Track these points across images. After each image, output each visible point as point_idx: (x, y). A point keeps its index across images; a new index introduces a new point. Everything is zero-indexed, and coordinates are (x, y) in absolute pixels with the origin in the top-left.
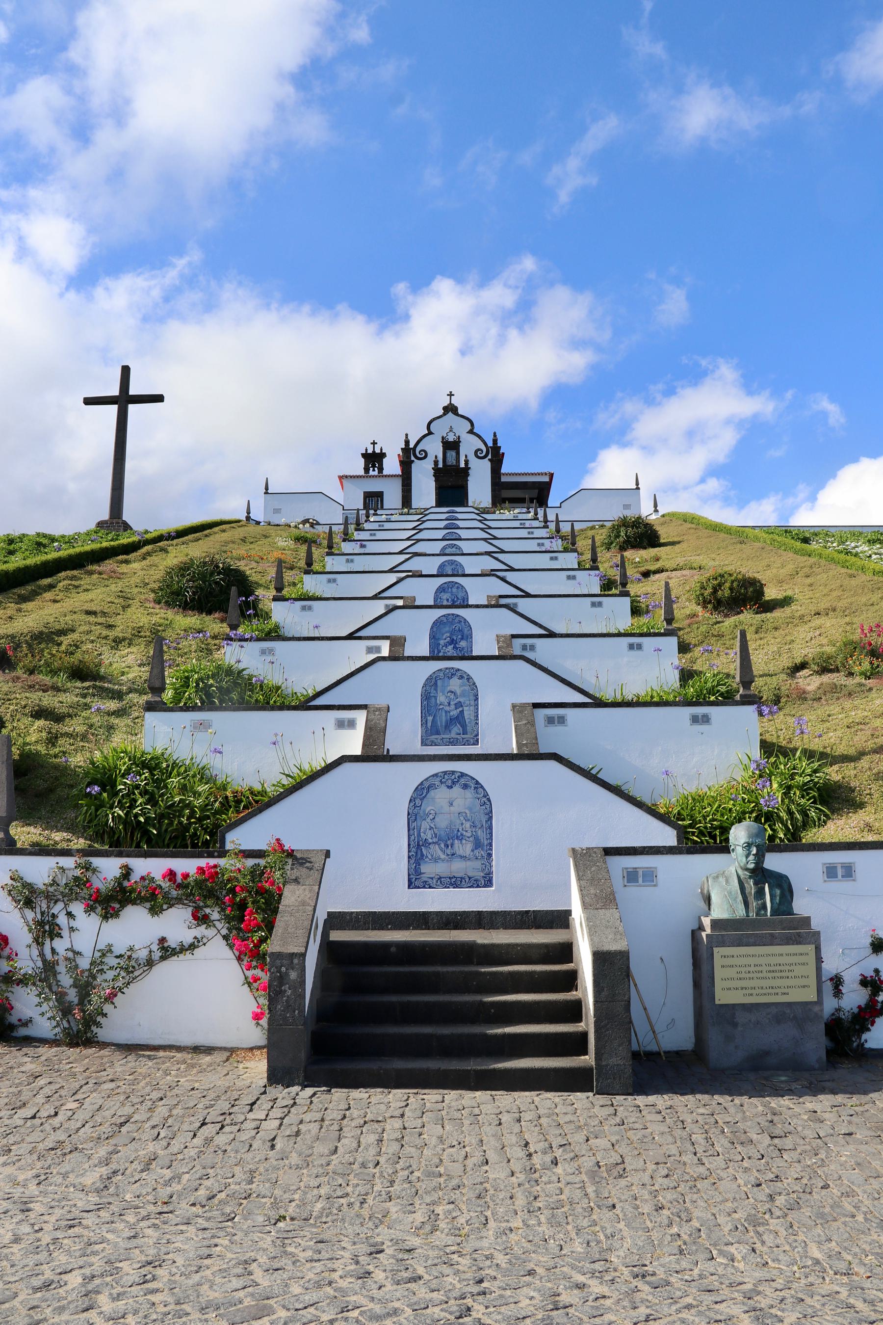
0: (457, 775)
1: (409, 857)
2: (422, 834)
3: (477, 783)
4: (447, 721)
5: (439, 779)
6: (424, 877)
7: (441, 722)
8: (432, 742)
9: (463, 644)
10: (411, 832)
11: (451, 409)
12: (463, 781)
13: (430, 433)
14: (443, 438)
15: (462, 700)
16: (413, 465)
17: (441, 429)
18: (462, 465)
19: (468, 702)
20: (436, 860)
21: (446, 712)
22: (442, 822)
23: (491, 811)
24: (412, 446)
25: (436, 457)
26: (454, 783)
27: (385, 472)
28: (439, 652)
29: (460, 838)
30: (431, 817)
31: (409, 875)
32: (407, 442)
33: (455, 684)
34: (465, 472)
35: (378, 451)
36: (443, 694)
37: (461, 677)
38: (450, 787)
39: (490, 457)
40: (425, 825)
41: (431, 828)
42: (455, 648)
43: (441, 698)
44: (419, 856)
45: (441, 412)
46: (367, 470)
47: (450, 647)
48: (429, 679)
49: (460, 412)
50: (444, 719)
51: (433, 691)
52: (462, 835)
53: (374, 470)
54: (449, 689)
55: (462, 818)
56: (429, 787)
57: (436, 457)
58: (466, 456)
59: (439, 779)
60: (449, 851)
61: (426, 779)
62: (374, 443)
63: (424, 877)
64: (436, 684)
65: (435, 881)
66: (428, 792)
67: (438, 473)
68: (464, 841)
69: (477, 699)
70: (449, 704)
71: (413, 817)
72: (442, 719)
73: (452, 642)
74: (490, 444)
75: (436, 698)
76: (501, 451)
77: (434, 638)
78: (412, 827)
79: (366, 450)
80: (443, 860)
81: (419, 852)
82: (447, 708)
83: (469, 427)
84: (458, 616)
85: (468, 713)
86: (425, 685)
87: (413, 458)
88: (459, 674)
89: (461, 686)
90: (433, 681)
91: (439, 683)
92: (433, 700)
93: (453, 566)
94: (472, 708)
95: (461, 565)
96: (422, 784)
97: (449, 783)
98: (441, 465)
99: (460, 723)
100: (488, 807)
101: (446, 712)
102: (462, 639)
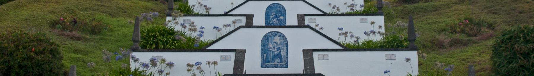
4: (273, 56)
7: (270, 57)
8: (266, 66)
9: (282, 18)
15: (280, 46)
19: (283, 48)
21: (273, 52)
28: (270, 21)
33: (277, 39)
36: (271, 44)
37: (280, 36)
42: (278, 20)
43: (270, 46)
47: (275, 19)
48: (265, 36)
50: (272, 56)
54: (274, 41)
64: (268, 39)
69: (287, 46)
70: (274, 48)
72: (271, 55)
73: (276, 17)
75: (268, 45)
77: (267, 14)
82: (273, 50)
84: (279, 4)
85: (283, 53)
86: (263, 39)
88: (279, 34)
89: (280, 40)
90: (267, 37)
91: (270, 38)
94: (285, 50)
99: (279, 57)
101: (273, 52)
102: (281, 15)
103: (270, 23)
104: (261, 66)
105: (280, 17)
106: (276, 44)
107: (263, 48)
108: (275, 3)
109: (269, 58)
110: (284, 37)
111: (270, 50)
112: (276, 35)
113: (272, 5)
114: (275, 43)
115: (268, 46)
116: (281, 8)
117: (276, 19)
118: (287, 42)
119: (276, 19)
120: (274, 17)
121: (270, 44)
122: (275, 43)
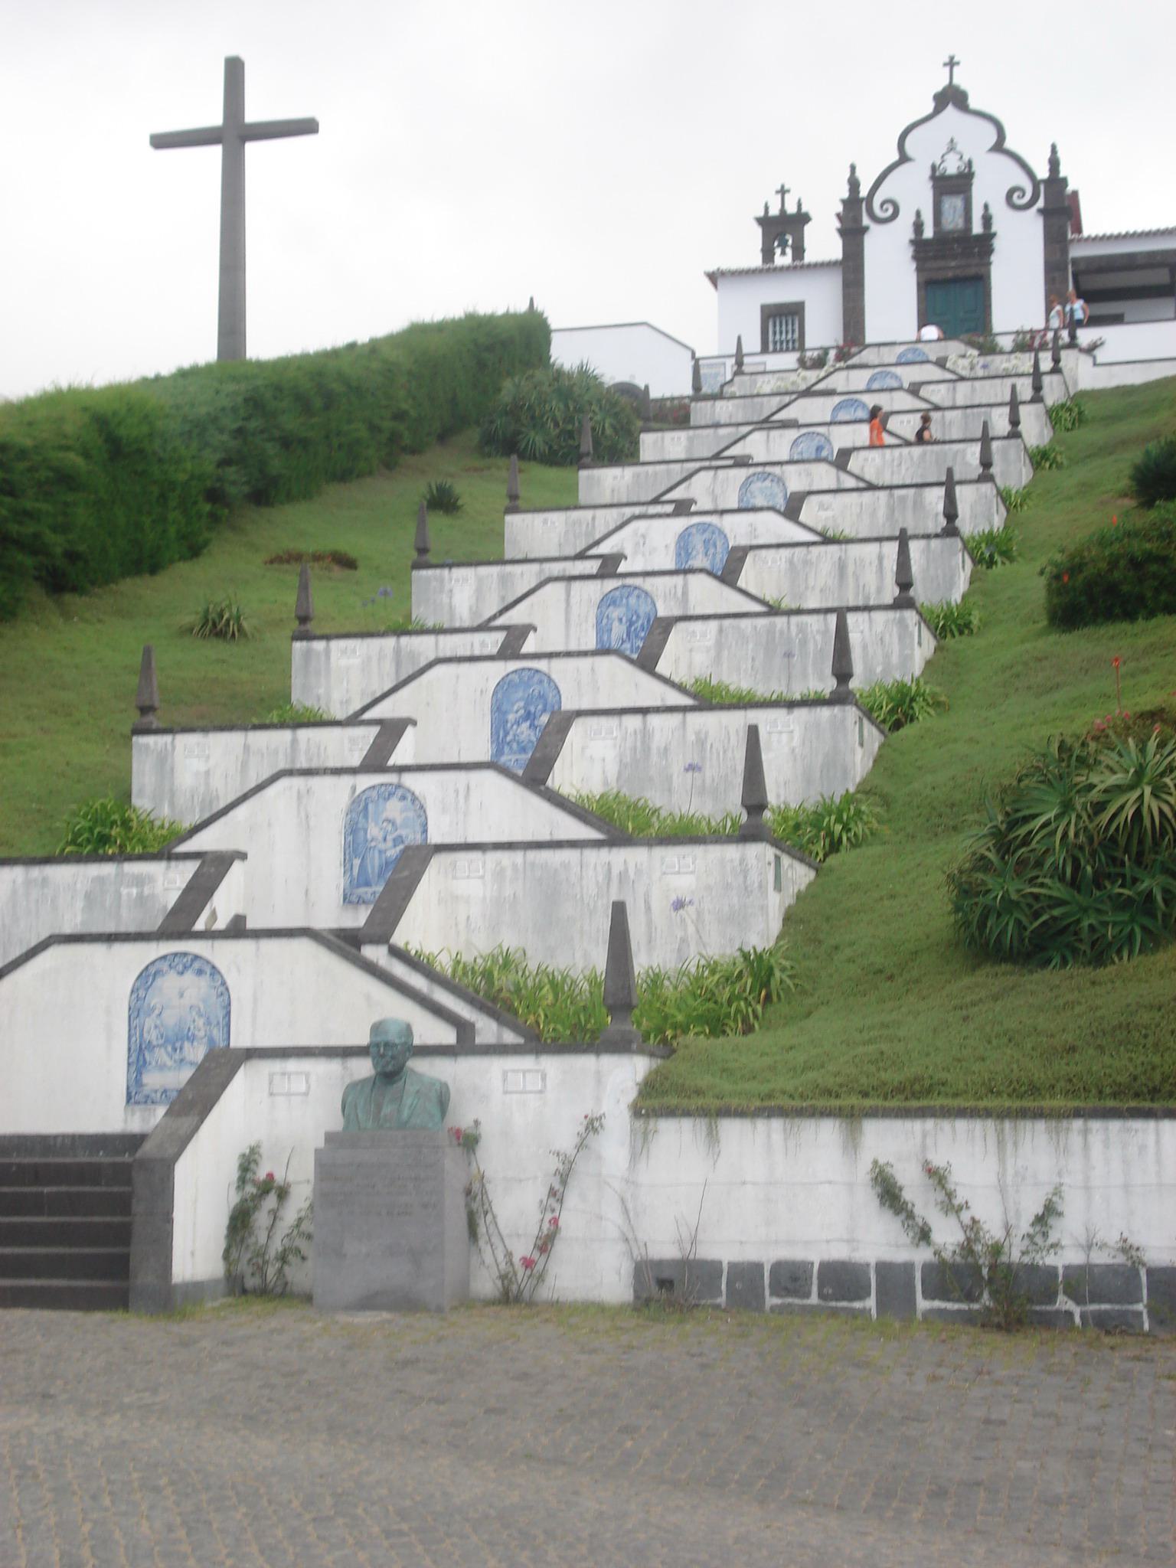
0: (190, 958)
1: (129, 1064)
2: (145, 1035)
3: (214, 967)
4: (381, 867)
5: (167, 963)
6: (146, 1090)
7: (373, 867)
10: (133, 1032)
11: (951, 98)
12: (196, 965)
13: (904, 158)
14: (934, 168)
16: (869, 241)
17: (927, 149)
18: (977, 228)
20: (162, 1067)
21: (380, 852)
22: (170, 1019)
23: (230, 1004)
24: (864, 192)
25: (918, 214)
26: (186, 968)
27: (809, 257)
28: (506, 734)
29: (192, 1039)
30: (157, 1012)
31: (128, 1088)
32: (854, 184)
33: (394, 808)
34: (983, 245)
35: (791, 209)
36: (376, 824)
37: (403, 798)
38: (182, 973)
39: (1041, 203)
40: (149, 1023)
41: (156, 1027)
42: (532, 726)
43: (374, 831)
44: (141, 1063)
45: (930, 107)
46: (768, 254)
47: (525, 725)
49: (973, 103)
50: (377, 862)
51: (361, 820)
52: (193, 1035)
53: (783, 253)
54: (384, 816)
55: (194, 1013)
56: (155, 974)
57: (918, 214)
58: (986, 207)
59: (167, 963)
60: (177, 1056)
61: (153, 963)
62: (783, 192)
63: (146, 1090)
64: (366, 808)
65: (159, 1094)
66: (154, 980)
67: (924, 251)
68: (195, 1044)
70: (385, 839)
71: (136, 1012)
74: (1042, 172)
76: (1070, 188)
78: (133, 1026)
79: (767, 209)
80: (170, 1069)
81: (141, 1058)
82: (382, 846)
83: (992, 138)
84: (537, 671)
86: (350, 811)
87: (866, 221)
89: (402, 812)
90: (362, 804)
91: (371, 807)
92: (362, 833)
93: (707, 535)
95: (721, 532)
96: (147, 968)
97: (180, 967)
98: (928, 233)
100: (226, 998)
101: (380, 852)
103: (509, 738)
104: (344, 899)
105: (540, 716)
106: (390, 825)
107: (350, 838)
108: (523, 669)
109: (370, 871)
110: (417, 802)
111: (373, 844)
112: (391, 795)
113: (513, 675)
114: (388, 820)
115: (366, 833)
116: (546, 684)
117: (528, 723)
118: (426, 818)
119: (528, 723)
120: (521, 717)
121: (373, 824)
122: (390, 821)
